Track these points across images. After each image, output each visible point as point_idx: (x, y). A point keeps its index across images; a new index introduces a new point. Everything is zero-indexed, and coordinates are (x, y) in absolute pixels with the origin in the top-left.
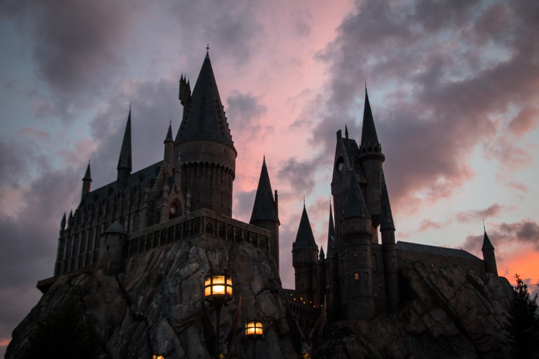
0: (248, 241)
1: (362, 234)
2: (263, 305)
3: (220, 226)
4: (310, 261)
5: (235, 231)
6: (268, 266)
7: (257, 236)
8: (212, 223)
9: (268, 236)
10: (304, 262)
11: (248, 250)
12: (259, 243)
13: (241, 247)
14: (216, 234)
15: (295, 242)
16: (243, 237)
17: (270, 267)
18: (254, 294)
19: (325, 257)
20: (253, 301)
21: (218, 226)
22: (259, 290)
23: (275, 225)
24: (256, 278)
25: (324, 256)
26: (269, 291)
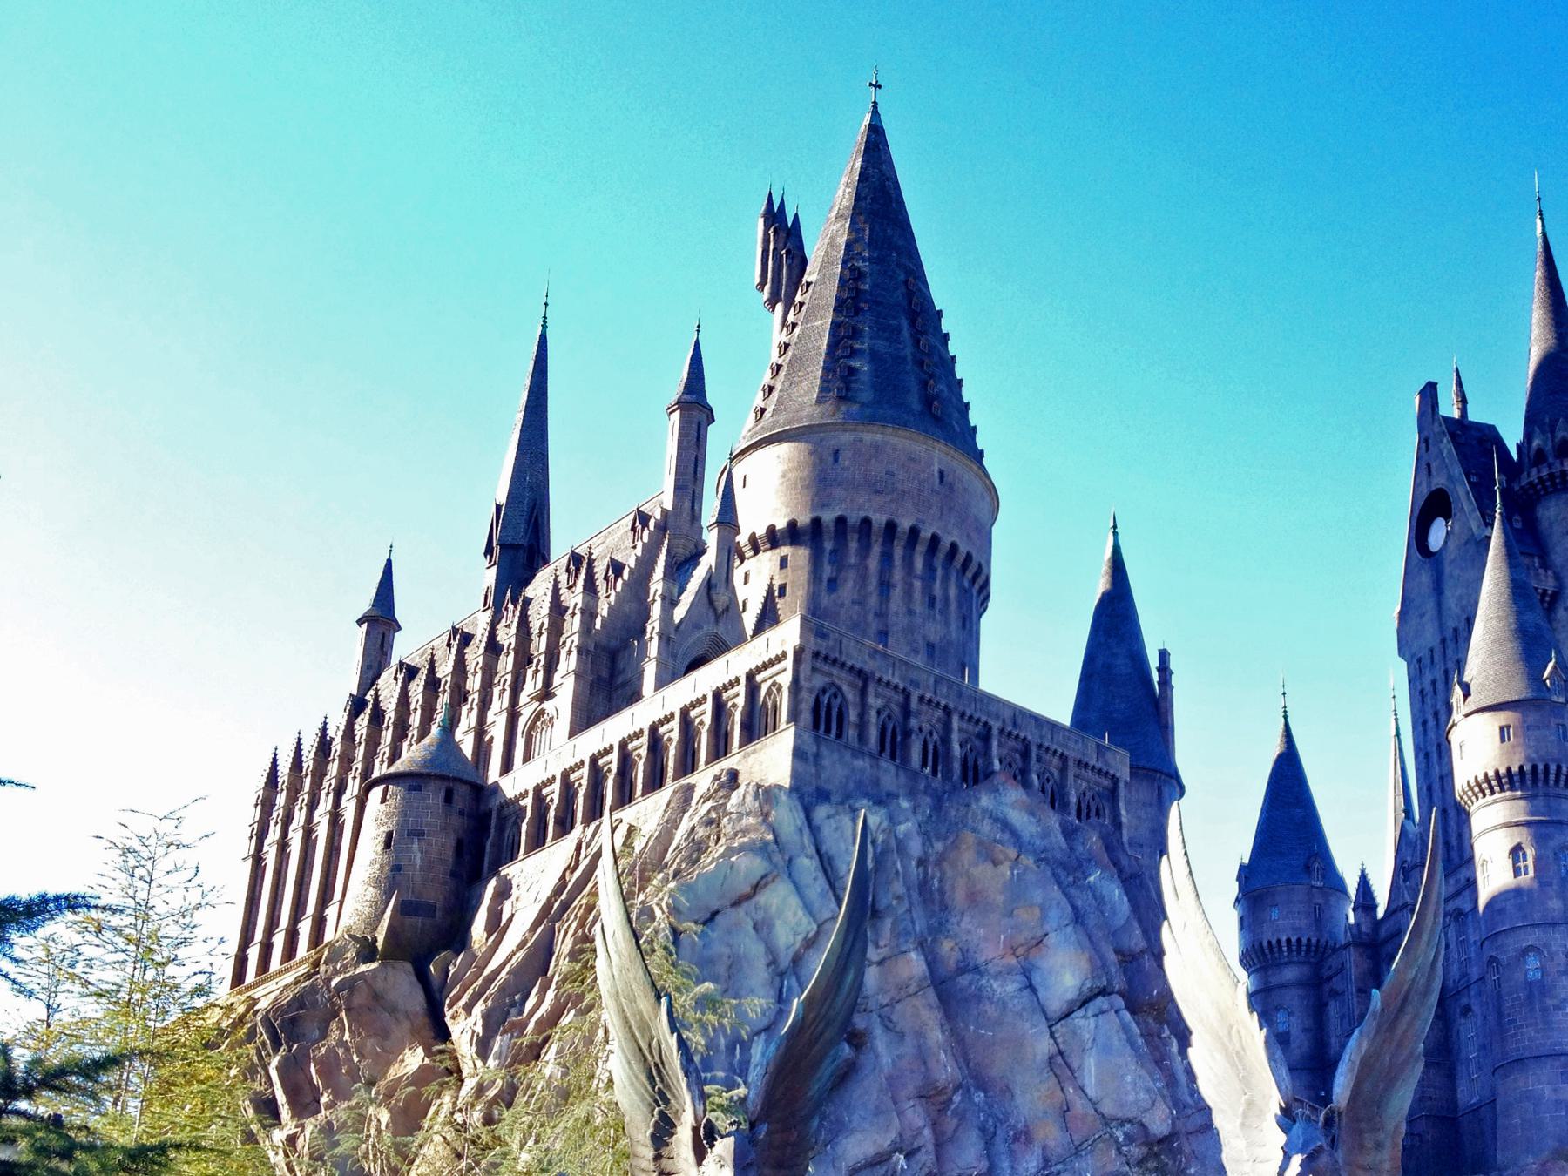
0: (1022, 778)
1: (1552, 777)
2: (1091, 1070)
3: (886, 706)
4: (1314, 940)
5: (955, 737)
6: (1115, 893)
7: (1063, 770)
8: (845, 688)
9: (1117, 775)
10: (1289, 941)
11: (1017, 818)
12: (1073, 799)
13: (985, 801)
14: (862, 737)
15: (1246, 861)
16: (997, 765)
17: (1125, 899)
18: (1044, 1012)
19: (1380, 913)
20: (1044, 1046)
21: (871, 700)
22: (1071, 995)
23: (1159, 788)
24: (1053, 938)
25: (1374, 907)
26: (1119, 1002)
